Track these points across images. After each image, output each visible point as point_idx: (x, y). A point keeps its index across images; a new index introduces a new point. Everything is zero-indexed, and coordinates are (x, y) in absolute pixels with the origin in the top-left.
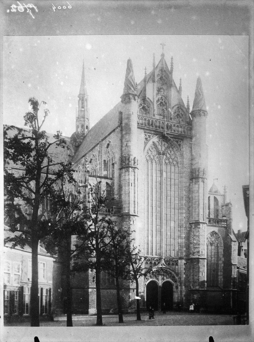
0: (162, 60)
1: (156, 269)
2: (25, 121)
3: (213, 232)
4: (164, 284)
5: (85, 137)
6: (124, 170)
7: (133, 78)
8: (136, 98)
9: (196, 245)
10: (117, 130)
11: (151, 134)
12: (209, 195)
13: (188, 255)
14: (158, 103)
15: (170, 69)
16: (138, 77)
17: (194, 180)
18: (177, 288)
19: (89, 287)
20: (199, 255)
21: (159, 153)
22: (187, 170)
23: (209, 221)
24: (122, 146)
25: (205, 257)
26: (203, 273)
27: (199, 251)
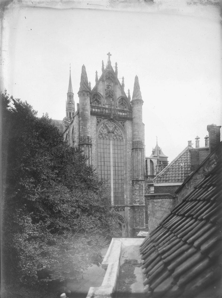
0: (109, 66)
10: (76, 117)
17: (134, 150)
18: (124, 226)
24: (79, 129)
26: (143, 216)
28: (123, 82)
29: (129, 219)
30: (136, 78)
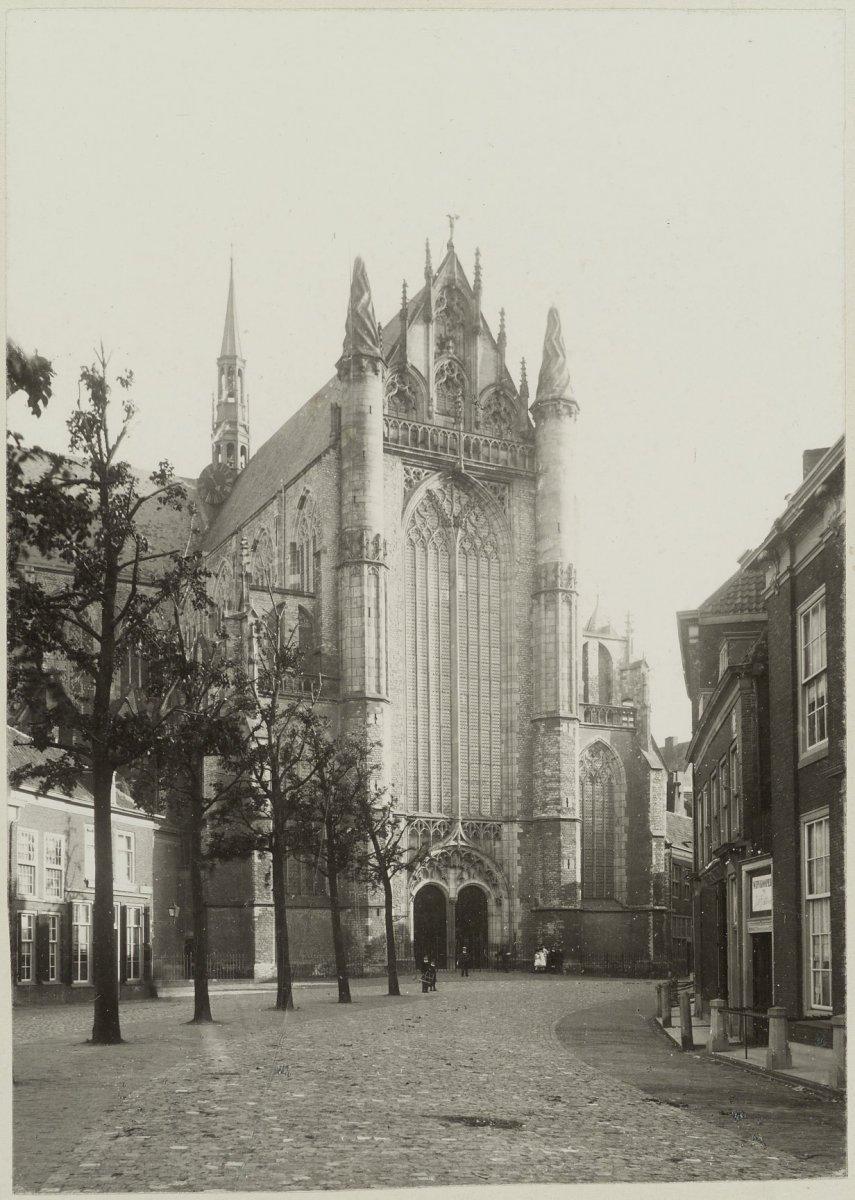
0: (451, 257)
1: (439, 851)
2: (70, 436)
3: (597, 743)
4: (462, 893)
5: (237, 478)
6: (347, 572)
7: (370, 309)
8: (380, 366)
9: (550, 781)
10: (328, 457)
11: (420, 470)
12: (585, 640)
13: (528, 810)
14: (440, 381)
15: (471, 283)
16: (385, 309)
17: (543, 596)
18: (499, 903)
19: (255, 902)
20: (559, 811)
21: (444, 523)
22: (522, 572)
23: (587, 714)
24: (340, 503)
25: (577, 815)
26: (572, 862)
27: (559, 799)
28: (502, 326)
29: (519, 870)
30: (553, 316)
